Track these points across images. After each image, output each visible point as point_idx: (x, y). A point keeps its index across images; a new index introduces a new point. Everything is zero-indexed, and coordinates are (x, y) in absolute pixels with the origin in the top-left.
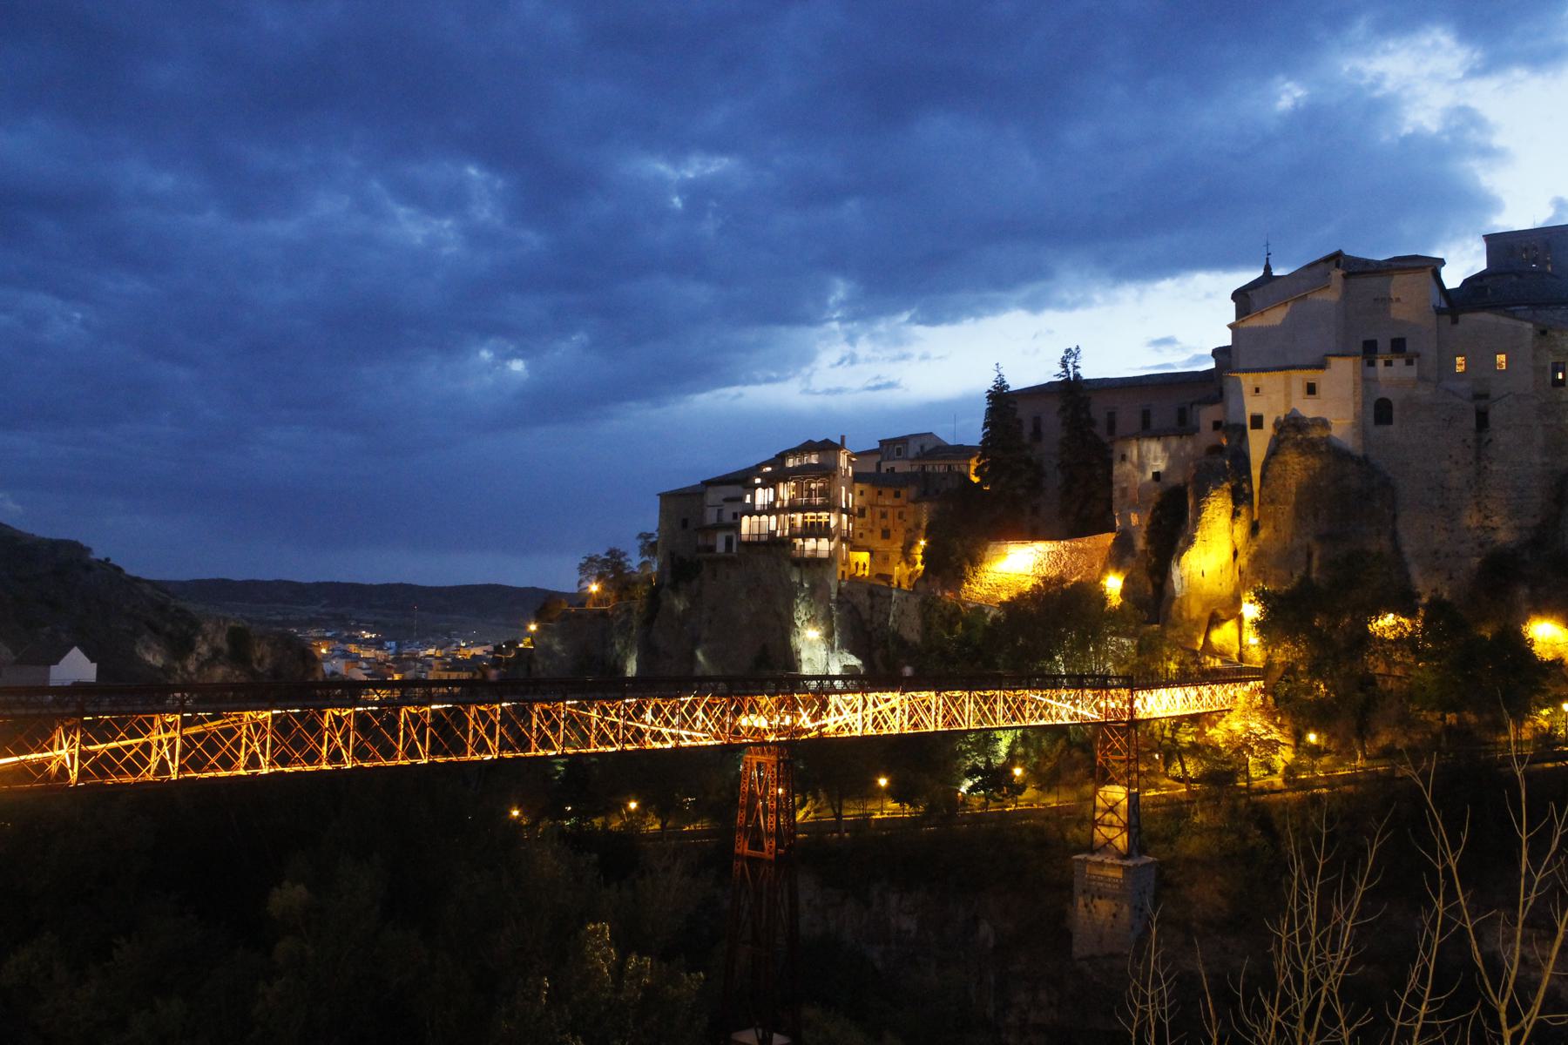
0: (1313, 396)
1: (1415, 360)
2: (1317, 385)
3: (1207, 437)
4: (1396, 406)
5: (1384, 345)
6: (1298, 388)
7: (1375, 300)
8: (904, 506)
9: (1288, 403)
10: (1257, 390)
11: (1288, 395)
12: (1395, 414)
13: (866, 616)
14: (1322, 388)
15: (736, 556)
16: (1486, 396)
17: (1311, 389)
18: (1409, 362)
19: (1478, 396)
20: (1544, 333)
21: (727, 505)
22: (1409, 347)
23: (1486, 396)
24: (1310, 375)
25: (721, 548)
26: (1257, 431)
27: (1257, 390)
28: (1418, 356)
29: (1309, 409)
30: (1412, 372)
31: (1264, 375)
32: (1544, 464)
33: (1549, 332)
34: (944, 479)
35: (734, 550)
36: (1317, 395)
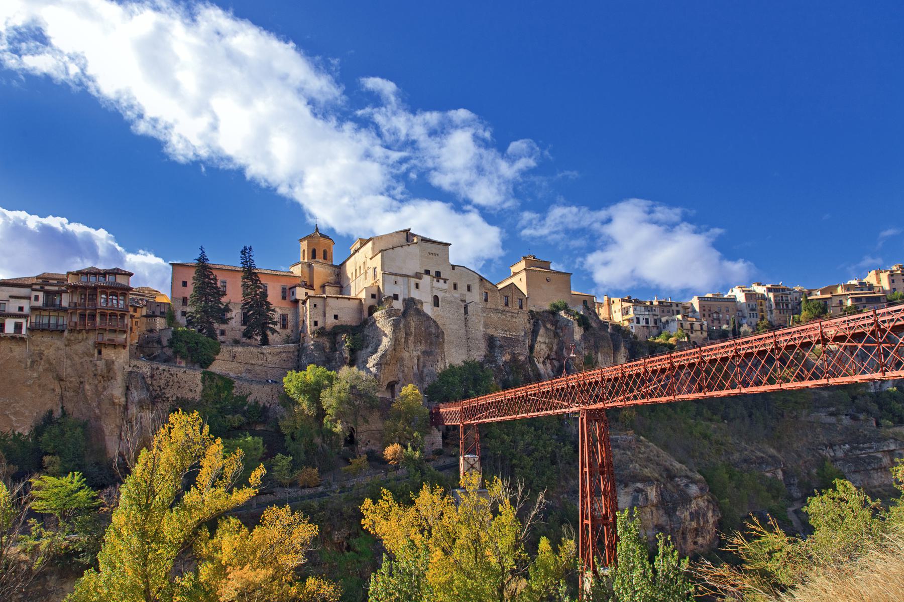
4: (440, 300)
8: (138, 318)
10: (396, 282)
12: (440, 303)
13: (149, 381)
14: (420, 286)
15: (26, 337)
17: (417, 286)
18: (445, 282)
21: (11, 300)
23: (465, 301)
24: (418, 281)
27: (396, 282)
28: (447, 280)
29: (415, 294)
30: (446, 286)
34: (158, 306)
35: (24, 331)
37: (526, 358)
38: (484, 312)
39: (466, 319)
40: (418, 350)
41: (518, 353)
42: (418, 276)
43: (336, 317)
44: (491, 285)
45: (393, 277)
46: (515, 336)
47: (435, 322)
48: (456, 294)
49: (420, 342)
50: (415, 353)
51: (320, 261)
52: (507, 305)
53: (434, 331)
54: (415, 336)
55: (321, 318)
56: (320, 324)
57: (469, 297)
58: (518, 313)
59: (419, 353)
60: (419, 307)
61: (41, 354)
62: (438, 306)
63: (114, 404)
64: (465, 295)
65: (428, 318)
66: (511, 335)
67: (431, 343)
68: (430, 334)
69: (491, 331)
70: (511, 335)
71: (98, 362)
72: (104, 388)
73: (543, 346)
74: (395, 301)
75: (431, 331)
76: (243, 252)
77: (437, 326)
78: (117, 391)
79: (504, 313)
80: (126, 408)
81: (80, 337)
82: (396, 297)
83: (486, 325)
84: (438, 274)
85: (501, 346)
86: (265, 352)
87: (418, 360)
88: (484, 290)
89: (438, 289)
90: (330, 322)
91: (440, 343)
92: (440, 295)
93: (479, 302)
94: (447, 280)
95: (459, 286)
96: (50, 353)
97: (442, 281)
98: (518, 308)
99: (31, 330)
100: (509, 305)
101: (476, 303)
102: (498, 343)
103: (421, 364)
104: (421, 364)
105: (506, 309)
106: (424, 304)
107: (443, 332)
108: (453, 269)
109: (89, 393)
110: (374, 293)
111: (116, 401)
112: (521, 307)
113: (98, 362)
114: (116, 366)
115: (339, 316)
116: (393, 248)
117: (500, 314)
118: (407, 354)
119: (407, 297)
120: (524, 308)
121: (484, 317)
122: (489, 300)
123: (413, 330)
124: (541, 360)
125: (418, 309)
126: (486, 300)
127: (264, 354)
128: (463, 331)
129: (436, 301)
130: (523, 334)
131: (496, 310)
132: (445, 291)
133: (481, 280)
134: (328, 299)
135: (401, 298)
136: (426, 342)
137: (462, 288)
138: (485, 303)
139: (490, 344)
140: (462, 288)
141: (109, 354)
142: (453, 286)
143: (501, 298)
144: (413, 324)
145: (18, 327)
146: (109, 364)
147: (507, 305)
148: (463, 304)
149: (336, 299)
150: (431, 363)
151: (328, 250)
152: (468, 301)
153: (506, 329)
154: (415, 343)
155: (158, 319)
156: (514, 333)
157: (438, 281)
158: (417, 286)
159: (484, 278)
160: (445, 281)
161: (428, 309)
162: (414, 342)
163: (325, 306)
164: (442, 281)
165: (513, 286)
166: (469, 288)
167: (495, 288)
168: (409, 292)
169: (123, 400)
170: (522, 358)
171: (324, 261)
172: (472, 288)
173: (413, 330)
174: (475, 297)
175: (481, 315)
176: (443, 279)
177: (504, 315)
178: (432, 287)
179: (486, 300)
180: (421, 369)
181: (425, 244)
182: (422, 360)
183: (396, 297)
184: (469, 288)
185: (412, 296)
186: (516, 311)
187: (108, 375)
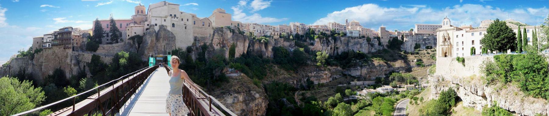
3: (146, 27)
5: (173, 16)
6: (163, 20)
9: (161, 22)
10: (156, 20)
11: (161, 21)
13: (78, 57)
14: (166, 20)
16: (186, 25)
17: (165, 20)
18: (177, 18)
19: (185, 24)
22: (176, 16)
23: (186, 25)
24: (165, 19)
25: (47, 46)
26: (156, 26)
27: (156, 20)
29: (164, 23)
30: (177, 20)
31: (157, 18)
35: (50, 46)
42: (166, 17)
43: (135, 33)
45: (155, 18)
47: (172, 33)
48: (182, 23)
49: (165, 40)
51: (140, 14)
52: (203, 25)
53: (171, 36)
54: (163, 38)
55: (130, 34)
56: (130, 36)
57: (187, 23)
58: (207, 28)
60: (165, 28)
61: (54, 52)
63: (68, 64)
65: (169, 31)
69: (196, 35)
71: (65, 53)
72: (66, 60)
73: (217, 40)
74: (155, 27)
78: (68, 61)
80: (71, 65)
81: (61, 46)
82: (156, 25)
83: (194, 33)
84: (175, 16)
85: (199, 40)
86: (114, 46)
87: (164, 46)
89: (174, 21)
90: (133, 35)
91: (174, 40)
95: (183, 20)
96: (56, 51)
99: (52, 45)
102: (198, 39)
104: (165, 48)
108: (182, 13)
109: (63, 61)
110: (148, 24)
111: (69, 63)
112: (209, 26)
113: (65, 53)
114: (69, 54)
116: (156, 8)
118: (160, 45)
119: (160, 25)
123: (162, 36)
124: (216, 44)
126: (195, 24)
127: (113, 46)
129: (173, 25)
130: (209, 35)
131: (199, 27)
132: (177, 22)
134: (133, 27)
135: (158, 25)
136: (168, 40)
137: (185, 20)
138: (194, 25)
140: (185, 20)
141: (67, 50)
144: (162, 34)
145: (49, 44)
146: (67, 53)
148: (185, 26)
151: (143, 10)
154: (163, 40)
155: (84, 38)
156: (205, 35)
157: (174, 18)
158: (165, 20)
160: (177, 18)
161: (169, 28)
163: (132, 29)
164: (176, 18)
166: (188, 20)
168: (161, 22)
169: (70, 63)
170: (208, 44)
171: (142, 14)
172: (189, 20)
173: (162, 36)
174: (190, 23)
178: (171, 20)
179: (195, 24)
180: (165, 49)
181: (170, 6)
182: (165, 46)
183: (156, 25)
184: (188, 20)
185: (163, 24)
187: (67, 57)
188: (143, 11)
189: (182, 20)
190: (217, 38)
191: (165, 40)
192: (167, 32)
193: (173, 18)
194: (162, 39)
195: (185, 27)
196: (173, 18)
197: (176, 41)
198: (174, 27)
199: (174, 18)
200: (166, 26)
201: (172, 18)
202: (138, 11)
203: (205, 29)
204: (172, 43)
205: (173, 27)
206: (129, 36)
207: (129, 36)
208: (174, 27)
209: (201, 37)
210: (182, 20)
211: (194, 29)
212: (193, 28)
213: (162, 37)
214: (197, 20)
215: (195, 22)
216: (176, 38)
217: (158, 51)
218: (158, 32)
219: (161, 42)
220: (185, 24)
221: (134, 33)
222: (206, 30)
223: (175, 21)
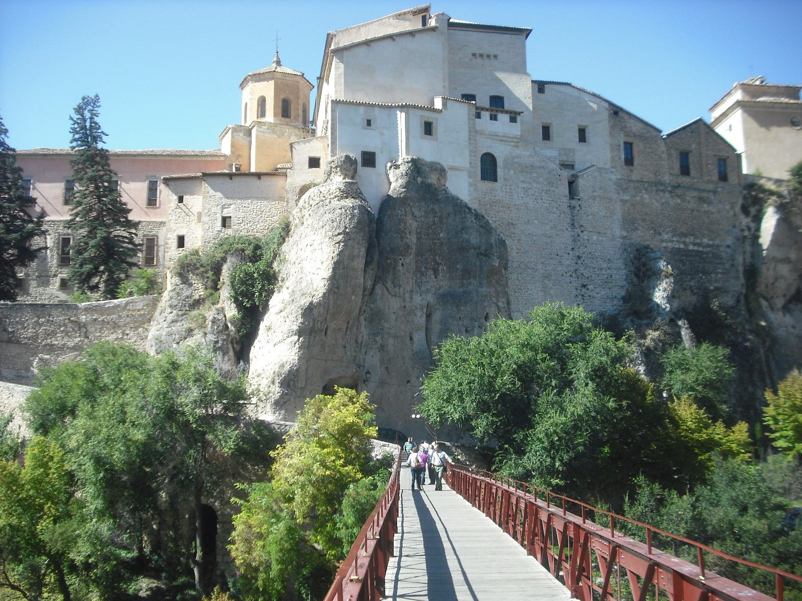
0: (429, 137)
1: (518, 118)
2: (434, 125)
4: (500, 163)
5: (483, 101)
7: (474, 55)
10: (369, 123)
18: (513, 120)
19: (565, 166)
20: (616, 113)
22: (507, 106)
23: (572, 167)
26: (368, 169)
27: (369, 123)
28: (519, 113)
30: (515, 130)
31: (377, 110)
32: (624, 238)
33: (620, 114)
36: (434, 136)
37: (738, 301)
38: (625, 190)
39: (572, 208)
40: (428, 291)
41: (716, 289)
43: (225, 222)
44: (641, 125)
45: (362, 110)
46: (708, 246)
47: (478, 216)
48: (550, 152)
49: (436, 272)
50: (417, 299)
52: (685, 170)
53: (474, 238)
54: (420, 253)
57: (583, 156)
58: (715, 192)
59: (430, 298)
60: (433, 179)
62: (495, 179)
64: (570, 150)
65: (460, 207)
66: (699, 245)
67: (467, 273)
68: (463, 248)
70: (699, 245)
75: (468, 241)
76: (79, 110)
77: (486, 228)
79: (679, 191)
83: (629, 223)
87: (429, 316)
88: (621, 139)
89: (494, 136)
92: (500, 152)
93: (608, 165)
94: (519, 113)
95: (554, 131)
97: (503, 118)
98: (715, 178)
100: (693, 172)
101: (600, 170)
103: (436, 327)
104: (436, 327)
105: (685, 180)
106: (449, 173)
107: (502, 243)
112: (723, 177)
115: (234, 221)
117: (667, 195)
120: (732, 178)
121: (624, 202)
122: (636, 162)
123: (412, 239)
124: (780, 302)
125: (429, 186)
128: (566, 237)
131: (657, 185)
133: (616, 113)
139: (638, 269)
142: (541, 130)
143: (670, 155)
144: (412, 224)
147: (685, 170)
148: (566, 174)
149: (227, 179)
150: (466, 322)
151: (291, 97)
152: (578, 167)
153: (684, 230)
156: (705, 241)
157: (494, 118)
159: (621, 109)
162: (418, 270)
164: (503, 118)
165: (702, 130)
166: (582, 135)
167: (654, 133)
172: (588, 135)
175: (615, 196)
176: (507, 112)
177: (679, 196)
178: (474, 133)
179: (629, 161)
181: (460, 34)
182: (437, 316)
184: (582, 135)
186: (711, 187)
188: (293, 106)
189: (546, 133)
190: (787, 260)
191: (436, 272)
192: (450, 209)
193: (486, 115)
194: (410, 259)
195: (571, 183)
196: (486, 115)
197: (513, 279)
198: (495, 180)
199: (494, 118)
200: (441, 171)
201: (478, 116)
202: (262, 102)
203: (702, 200)
204: (483, 290)
205: (484, 178)
206: (181, 242)
207: (181, 242)
208: (495, 180)
209: (679, 249)
210: (546, 133)
211: (627, 198)
212: (622, 186)
213: (413, 250)
214: (642, 138)
215: (629, 146)
216: (513, 254)
217: (382, 348)
218: (380, 213)
219: (408, 288)
220: (565, 166)
221: (219, 223)
222: (710, 203)
223: (504, 139)
